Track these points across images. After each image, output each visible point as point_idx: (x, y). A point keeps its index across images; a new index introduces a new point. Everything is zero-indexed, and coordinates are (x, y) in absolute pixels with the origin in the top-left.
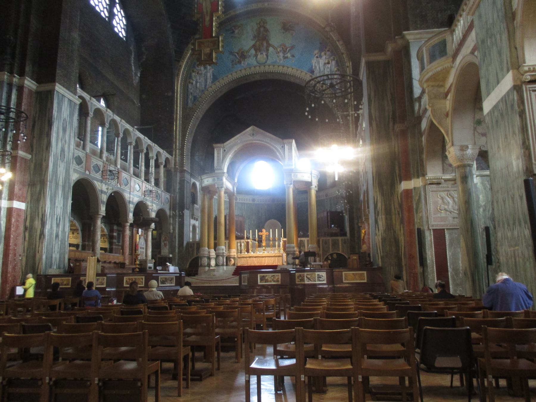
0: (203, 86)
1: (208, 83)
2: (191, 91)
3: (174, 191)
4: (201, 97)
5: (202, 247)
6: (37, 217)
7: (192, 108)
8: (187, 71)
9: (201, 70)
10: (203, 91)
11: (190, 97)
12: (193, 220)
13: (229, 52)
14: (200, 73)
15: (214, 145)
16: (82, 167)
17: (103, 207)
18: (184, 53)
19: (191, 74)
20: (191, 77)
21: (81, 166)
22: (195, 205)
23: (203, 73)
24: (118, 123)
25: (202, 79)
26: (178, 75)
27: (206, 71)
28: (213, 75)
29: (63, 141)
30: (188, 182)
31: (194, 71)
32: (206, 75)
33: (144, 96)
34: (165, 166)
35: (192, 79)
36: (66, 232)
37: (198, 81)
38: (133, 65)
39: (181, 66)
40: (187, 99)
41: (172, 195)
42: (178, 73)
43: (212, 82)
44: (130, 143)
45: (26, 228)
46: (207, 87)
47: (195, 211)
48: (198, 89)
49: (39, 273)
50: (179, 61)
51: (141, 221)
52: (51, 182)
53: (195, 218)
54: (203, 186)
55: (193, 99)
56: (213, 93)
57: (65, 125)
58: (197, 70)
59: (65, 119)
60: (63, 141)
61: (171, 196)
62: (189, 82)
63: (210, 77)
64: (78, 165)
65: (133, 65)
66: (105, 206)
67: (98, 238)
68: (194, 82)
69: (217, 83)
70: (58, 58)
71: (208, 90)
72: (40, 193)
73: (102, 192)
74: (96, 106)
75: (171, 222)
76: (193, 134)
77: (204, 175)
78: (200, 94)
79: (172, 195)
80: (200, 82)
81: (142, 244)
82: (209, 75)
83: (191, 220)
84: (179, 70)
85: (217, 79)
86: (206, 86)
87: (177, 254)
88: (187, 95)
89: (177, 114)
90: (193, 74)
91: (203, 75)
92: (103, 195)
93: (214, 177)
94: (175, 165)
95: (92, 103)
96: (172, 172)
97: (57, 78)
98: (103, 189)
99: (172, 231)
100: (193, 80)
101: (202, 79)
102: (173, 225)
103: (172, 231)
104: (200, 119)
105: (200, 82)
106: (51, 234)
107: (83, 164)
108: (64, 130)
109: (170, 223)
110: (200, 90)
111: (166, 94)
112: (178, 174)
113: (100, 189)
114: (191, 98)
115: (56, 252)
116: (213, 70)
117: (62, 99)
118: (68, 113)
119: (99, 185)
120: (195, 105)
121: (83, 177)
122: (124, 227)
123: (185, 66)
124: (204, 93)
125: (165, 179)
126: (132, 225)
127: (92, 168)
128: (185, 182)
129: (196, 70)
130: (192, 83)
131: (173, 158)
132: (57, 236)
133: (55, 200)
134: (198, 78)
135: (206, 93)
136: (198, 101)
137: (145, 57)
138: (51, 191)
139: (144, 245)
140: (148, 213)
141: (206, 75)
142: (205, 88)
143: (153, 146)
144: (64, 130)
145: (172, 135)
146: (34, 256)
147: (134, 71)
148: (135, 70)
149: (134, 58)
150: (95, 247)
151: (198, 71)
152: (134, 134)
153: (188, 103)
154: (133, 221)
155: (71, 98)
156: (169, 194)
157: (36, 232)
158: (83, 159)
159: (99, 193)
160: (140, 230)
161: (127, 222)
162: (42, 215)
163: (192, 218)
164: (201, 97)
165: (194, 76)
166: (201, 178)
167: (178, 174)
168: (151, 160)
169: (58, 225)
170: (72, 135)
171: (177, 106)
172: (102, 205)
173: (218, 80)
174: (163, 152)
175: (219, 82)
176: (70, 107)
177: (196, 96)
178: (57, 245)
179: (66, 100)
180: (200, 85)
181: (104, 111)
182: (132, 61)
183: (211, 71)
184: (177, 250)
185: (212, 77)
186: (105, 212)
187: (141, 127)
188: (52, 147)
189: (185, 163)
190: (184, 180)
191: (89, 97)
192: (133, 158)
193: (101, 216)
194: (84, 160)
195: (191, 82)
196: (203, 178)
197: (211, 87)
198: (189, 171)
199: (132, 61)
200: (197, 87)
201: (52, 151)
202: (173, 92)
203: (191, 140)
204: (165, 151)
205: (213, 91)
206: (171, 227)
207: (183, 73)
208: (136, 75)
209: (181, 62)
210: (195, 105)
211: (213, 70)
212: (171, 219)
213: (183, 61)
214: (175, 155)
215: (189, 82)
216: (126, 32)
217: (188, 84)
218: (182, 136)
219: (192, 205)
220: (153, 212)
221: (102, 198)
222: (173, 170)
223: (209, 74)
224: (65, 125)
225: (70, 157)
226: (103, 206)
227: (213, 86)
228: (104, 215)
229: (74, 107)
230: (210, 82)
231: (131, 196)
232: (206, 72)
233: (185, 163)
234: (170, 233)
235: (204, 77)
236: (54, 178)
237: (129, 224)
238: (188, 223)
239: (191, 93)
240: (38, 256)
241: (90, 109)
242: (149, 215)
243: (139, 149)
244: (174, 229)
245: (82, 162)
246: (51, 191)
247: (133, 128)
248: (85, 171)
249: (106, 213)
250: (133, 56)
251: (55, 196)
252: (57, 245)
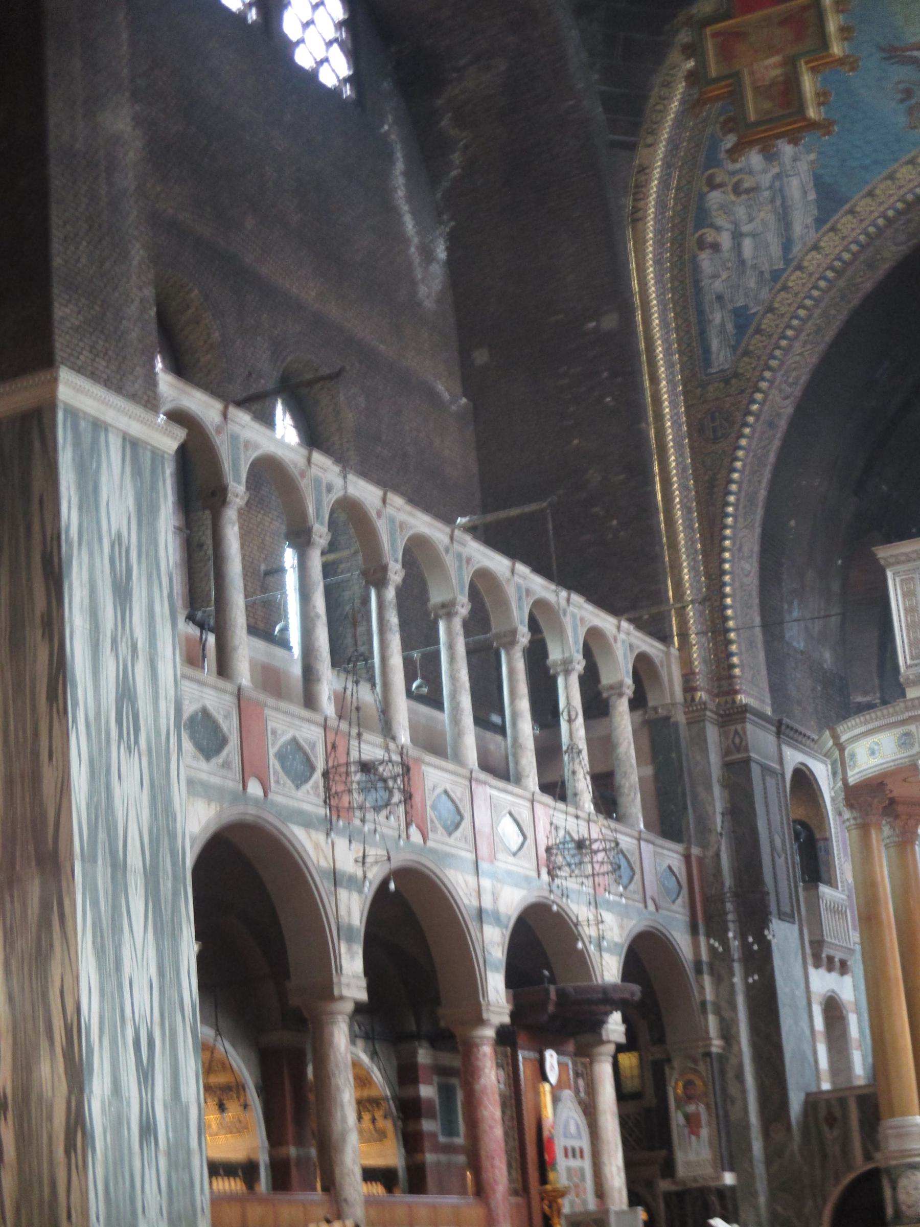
0: (776, 250)
1: (798, 229)
2: (718, 286)
3: (704, 828)
4: (770, 309)
5: (892, 1115)
6: (44, 1044)
7: (736, 375)
8: (678, 189)
9: (750, 173)
10: (776, 275)
11: (717, 317)
12: (822, 971)
13: (882, 49)
14: (746, 185)
15: (883, 553)
16: (226, 765)
17: (352, 957)
18: (652, 101)
19: (702, 197)
20: (702, 218)
21: (220, 759)
22: (824, 889)
23: (765, 180)
24: (373, 514)
25: (766, 215)
26: (637, 218)
27: (776, 170)
28: (819, 184)
29: (123, 649)
30: (766, 769)
31: (718, 180)
32: (781, 190)
33: (481, 357)
34: (638, 702)
35: (712, 226)
36: (187, 1107)
37: (746, 229)
38: (405, 208)
39: (644, 170)
40: (702, 332)
41: (695, 851)
42: (636, 210)
43: (820, 222)
44: (443, 606)
46: (797, 249)
47: (826, 917)
48: (749, 272)
50: (632, 147)
51: (551, 1008)
52: (90, 858)
53: (830, 959)
54: (852, 781)
55: (730, 327)
56: (830, 274)
57: (121, 567)
58: (733, 173)
59: (119, 536)
60: (123, 649)
61: (687, 858)
62: (701, 244)
63: (805, 193)
64: (208, 758)
65: (405, 208)
66: (360, 951)
67: (344, 1119)
68: (725, 240)
69: (847, 224)
70: (56, 246)
71: (800, 268)
72: (45, 923)
73: (336, 878)
74: (257, 446)
75: (709, 996)
76: (760, 512)
77: (851, 722)
78: (764, 294)
79: (695, 851)
80: (753, 235)
81: (573, 1129)
82: (794, 187)
83: (812, 971)
84: (640, 190)
85: (842, 201)
86: (787, 246)
87: (760, 1169)
88: (701, 312)
89: (659, 417)
90: (715, 198)
91: (766, 194)
92: (343, 894)
93: (903, 722)
94: (689, 688)
95: (234, 438)
96: (676, 724)
97: (60, 342)
98: (339, 866)
99: (716, 1045)
100: (718, 229)
101: (762, 214)
102: (718, 1012)
103: (716, 1045)
104: (783, 424)
105: (753, 235)
106: (118, 1123)
107: (232, 749)
108: (122, 593)
109: (703, 1004)
110: (762, 273)
111: (592, 324)
112: (712, 733)
113: (323, 864)
114: (723, 324)
115: (153, 1213)
116: (812, 156)
117: (95, 442)
118: (131, 502)
119: (317, 846)
120: (747, 353)
121: (233, 813)
122: (468, 1050)
123: (668, 165)
124: (785, 288)
125: (649, 771)
126: (505, 1037)
127: (274, 764)
128: (756, 771)
129: (726, 178)
130: (716, 247)
131: (674, 651)
132: (148, 1130)
133: (118, 947)
134: (741, 212)
135: (794, 279)
136: (758, 331)
137: (456, 158)
138: (95, 904)
139: (579, 1136)
140: (581, 962)
141: (779, 192)
142: (787, 261)
143: (563, 603)
144: (122, 593)
145: (651, 532)
147: (416, 240)
148: (418, 233)
149: (406, 174)
150: (337, 1171)
151: (735, 179)
152: (459, 556)
153: (707, 350)
154: (513, 1015)
155: (136, 429)
156: (679, 847)
157: (50, 1119)
158: (224, 726)
159: (324, 886)
160: (551, 1058)
161: (480, 1021)
163: (817, 966)
164: (770, 309)
165: (722, 207)
166: (835, 737)
167: (712, 733)
168: (560, 681)
169: (146, 1075)
170: (157, 608)
171: (655, 380)
172: (343, 948)
173: (847, 207)
174: (619, 628)
175: (852, 212)
176: (137, 472)
177: (746, 307)
178: (150, 1175)
179: (115, 445)
180: (756, 248)
181: (296, 465)
182: (401, 193)
183: (803, 167)
184: (757, 1147)
185: (812, 196)
186: (363, 983)
187: (490, 518)
188: (74, 687)
189: (737, 671)
190: (747, 761)
191: (218, 405)
192: (467, 685)
193: (349, 1007)
194: (230, 726)
195: (710, 236)
196: (844, 738)
197: (816, 247)
198: (769, 711)
199: (401, 193)
200: (742, 262)
201: (75, 704)
202: (626, 309)
203: (752, 542)
204: (625, 625)
205: (831, 268)
206: (712, 1021)
207: (661, 205)
208: (428, 255)
209: (642, 151)
210: (747, 353)
211: (812, 156)
212: (707, 980)
214: (684, 636)
215: (701, 244)
216: (354, 54)
217: (694, 257)
218: (702, 531)
219: (805, 889)
220: (606, 956)
221: (343, 911)
222: (680, 717)
223: (795, 182)
224: (121, 567)
225: (163, 721)
226: (349, 950)
227: (830, 243)
228: (363, 996)
229: (153, 471)
230: (809, 220)
231: (486, 883)
232: (778, 176)
233: (737, 671)
234: (708, 1054)
235: (773, 201)
236: (102, 836)
237: (489, 1033)
238: (800, 992)
239: (720, 298)
241: (227, 466)
242: (590, 979)
243: (494, 630)
244: (728, 1035)
245: (223, 742)
246: (95, 904)
247: (448, 530)
248: (245, 787)
249: (371, 989)
250: (400, 166)
251: (116, 929)
252: (150, 1175)
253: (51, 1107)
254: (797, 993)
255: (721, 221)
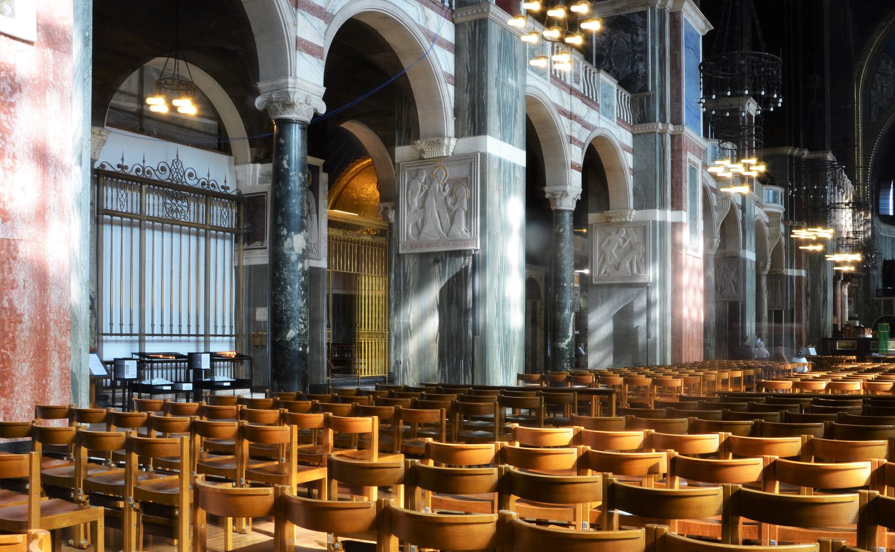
2: (875, 99)
37: (885, 85)
39: (861, 67)
45: (807, 295)
49: (825, 336)
55: (877, 111)
68: (879, 88)
89: (858, 132)
111: (844, 106)
130: (876, 89)
146: (819, 321)
157: (819, 298)
162: (824, 282)
171: (858, 123)
213: (864, 58)
239: (875, 102)
240: (822, 320)
253: (819, 296)
254: (874, 273)
255: (878, 83)
